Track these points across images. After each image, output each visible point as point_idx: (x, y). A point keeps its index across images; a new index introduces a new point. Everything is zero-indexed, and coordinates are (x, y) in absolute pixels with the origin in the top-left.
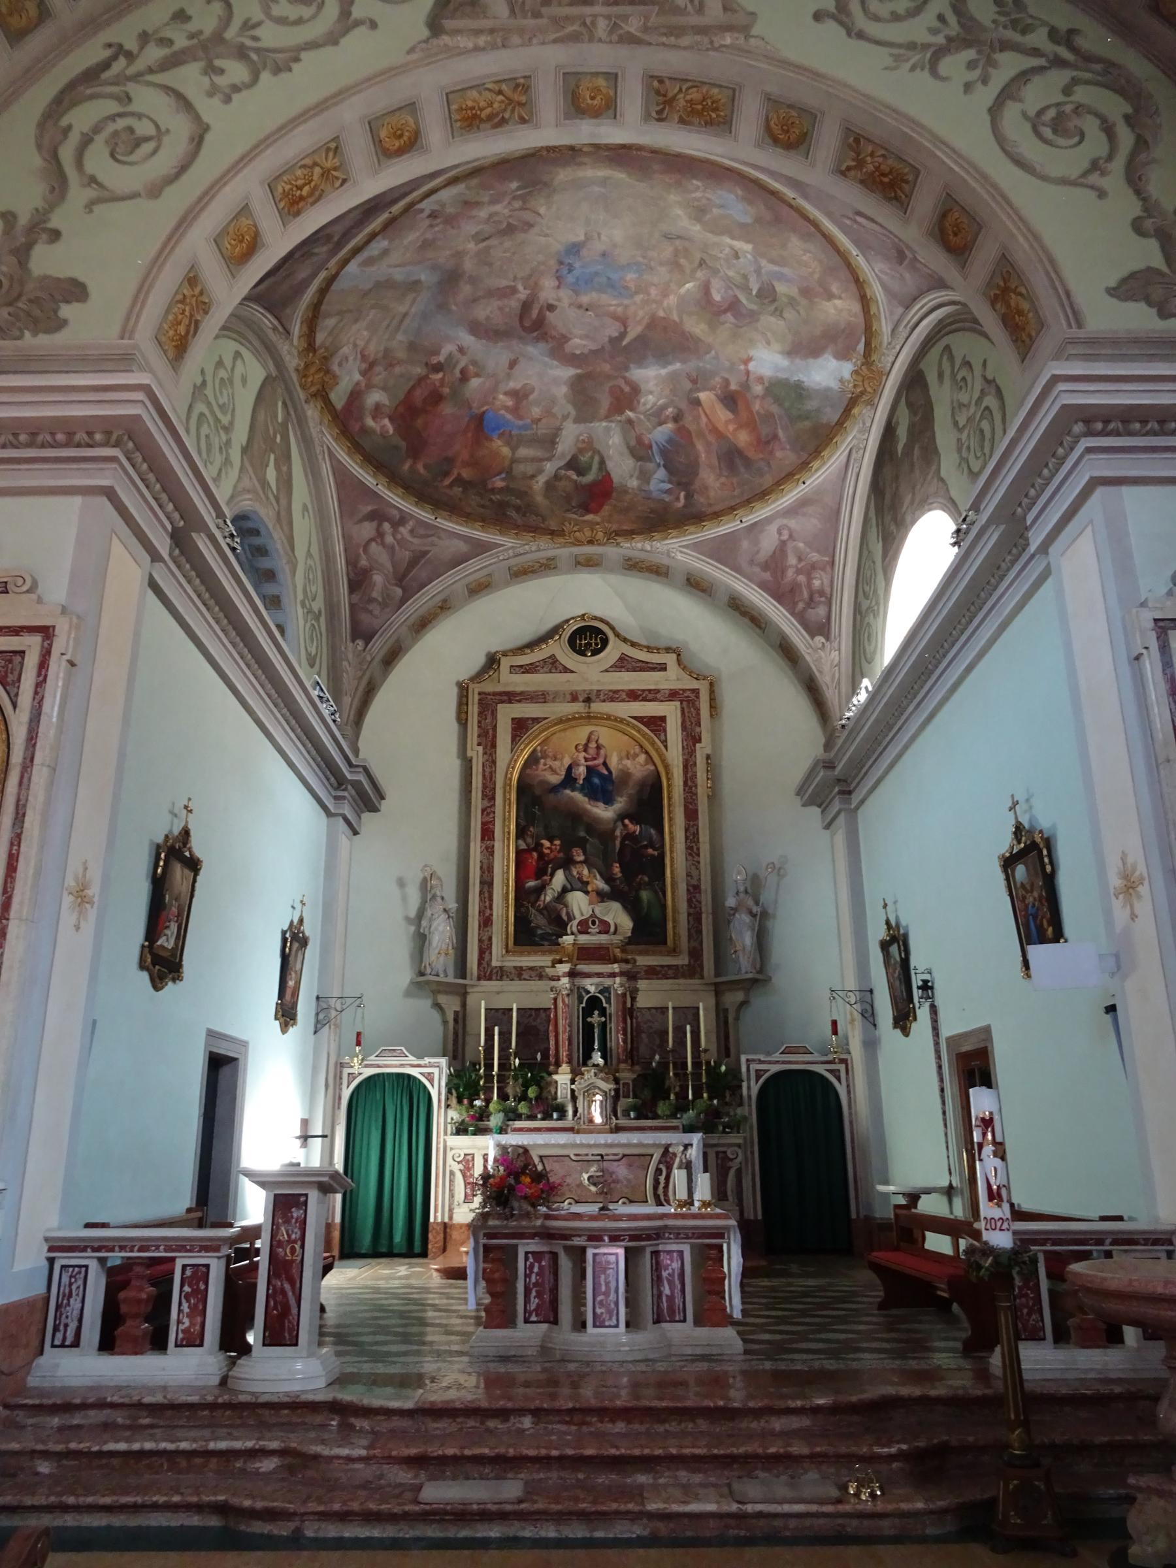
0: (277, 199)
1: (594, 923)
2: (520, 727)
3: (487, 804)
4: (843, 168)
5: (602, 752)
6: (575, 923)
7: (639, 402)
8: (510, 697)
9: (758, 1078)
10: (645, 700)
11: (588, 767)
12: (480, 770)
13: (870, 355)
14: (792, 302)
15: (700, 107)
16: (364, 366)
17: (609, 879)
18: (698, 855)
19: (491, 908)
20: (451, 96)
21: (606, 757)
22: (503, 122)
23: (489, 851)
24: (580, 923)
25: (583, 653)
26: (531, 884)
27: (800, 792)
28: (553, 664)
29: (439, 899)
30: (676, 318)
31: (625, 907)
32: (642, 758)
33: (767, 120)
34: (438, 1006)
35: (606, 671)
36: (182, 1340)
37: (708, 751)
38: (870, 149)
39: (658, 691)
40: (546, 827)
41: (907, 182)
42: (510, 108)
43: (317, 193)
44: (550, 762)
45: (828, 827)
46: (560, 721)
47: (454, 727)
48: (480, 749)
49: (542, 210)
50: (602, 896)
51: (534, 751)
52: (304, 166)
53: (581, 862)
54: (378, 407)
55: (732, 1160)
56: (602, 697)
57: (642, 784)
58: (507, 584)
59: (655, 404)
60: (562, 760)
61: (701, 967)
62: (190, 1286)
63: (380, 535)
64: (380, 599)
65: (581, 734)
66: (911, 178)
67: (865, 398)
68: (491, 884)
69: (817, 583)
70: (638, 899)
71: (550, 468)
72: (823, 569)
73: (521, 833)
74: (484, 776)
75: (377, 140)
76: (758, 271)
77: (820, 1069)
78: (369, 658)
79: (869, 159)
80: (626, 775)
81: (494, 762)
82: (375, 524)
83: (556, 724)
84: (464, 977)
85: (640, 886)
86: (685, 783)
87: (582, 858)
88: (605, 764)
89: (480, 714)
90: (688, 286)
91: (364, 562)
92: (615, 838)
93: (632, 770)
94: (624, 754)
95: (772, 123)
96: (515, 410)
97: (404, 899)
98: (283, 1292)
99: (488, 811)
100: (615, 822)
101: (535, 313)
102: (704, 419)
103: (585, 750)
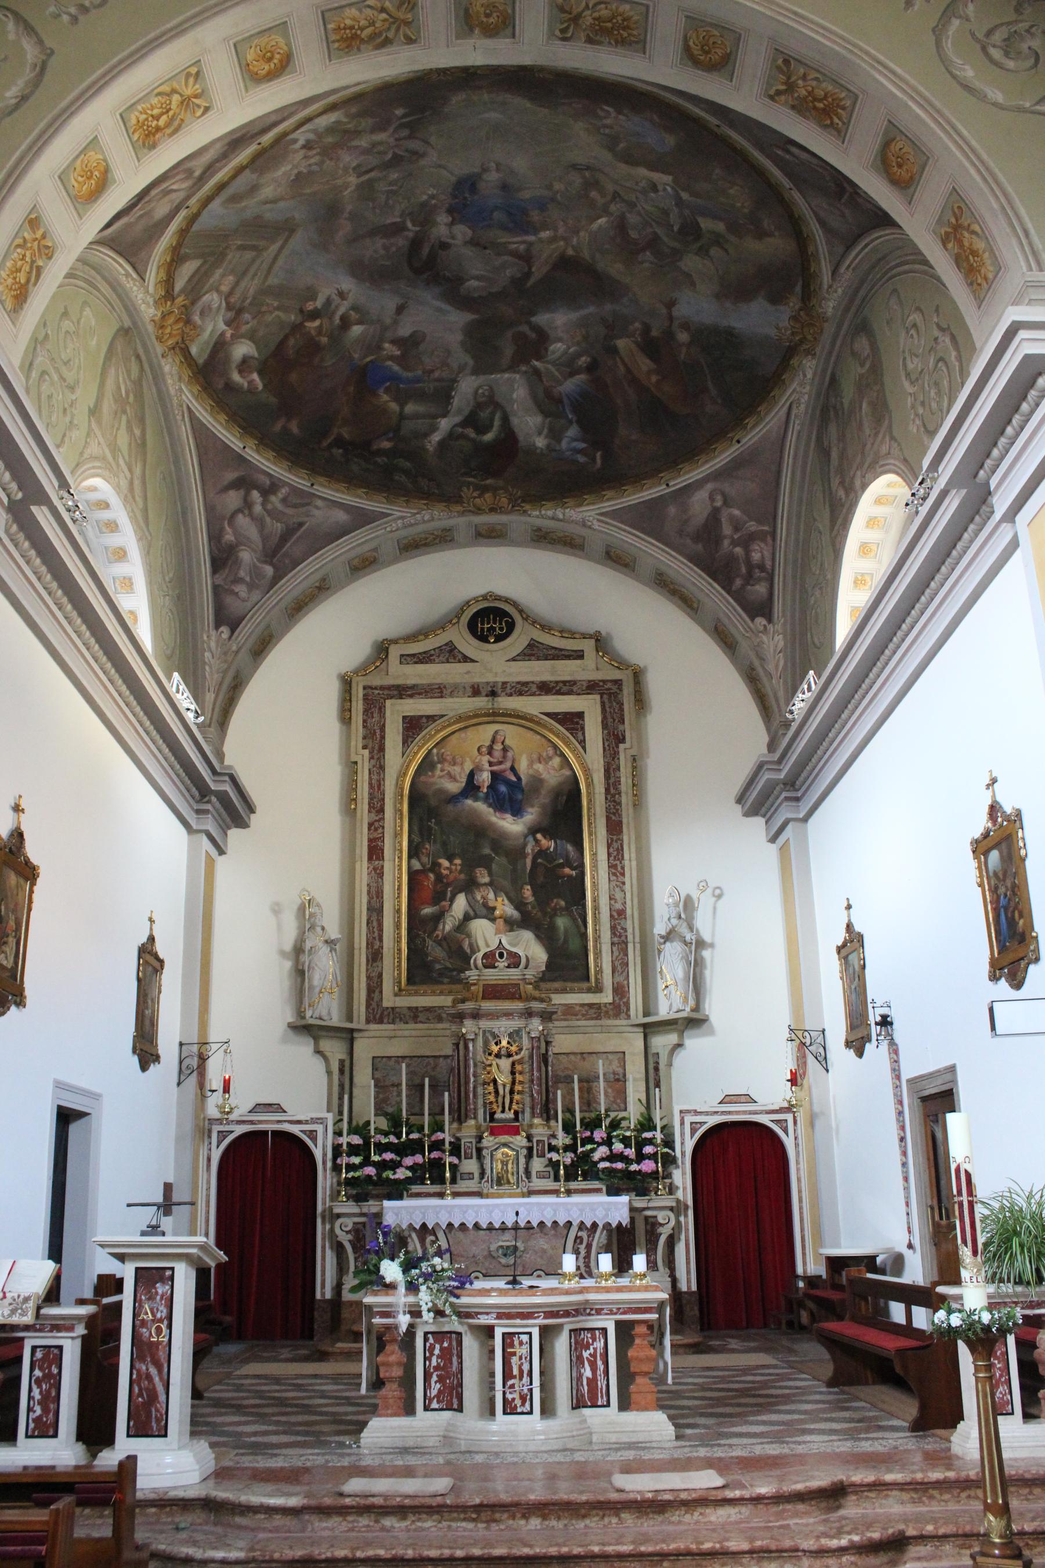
0: (131, 131)
1: (501, 955)
2: (413, 726)
3: (374, 817)
4: (772, 92)
5: (510, 754)
6: (480, 955)
7: (546, 350)
8: (402, 691)
9: (693, 1131)
10: (559, 693)
11: (493, 773)
12: (366, 777)
13: (809, 300)
14: (718, 240)
15: (609, 25)
16: (230, 315)
17: (519, 904)
18: (623, 874)
19: (381, 940)
20: (327, 15)
21: (513, 761)
22: (387, 42)
23: (378, 873)
24: (486, 956)
25: (484, 639)
26: (427, 910)
27: (740, 800)
28: (450, 653)
29: (319, 929)
30: (586, 254)
31: (538, 937)
32: (557, 761)
33: (686, 39)
34: (318, 1052)
35: (513, 659)
36: (34, 1430)
37: (633, 752)
38: (802, 71)
39: (574, 683)
40: (444, 844)
41: (844, 108)
42: (394, 27)
43: (176, 123)
44: (448, 768)
45: (773, 840)
46: (460, 719)
47: (334, 726)
48: (366, 752)
49: (433, 140)
50: (511, 925)
51: (430, 752)
52: (159, 94)
53: (485, 884)
54: (245, 360)
55: (662, 1225)
56: (508, 691)
57: (557, 793)
58: (395, 560)
59: (566, 352)
61: (627, 1005)
62: (40, 1369)
63: (248, 505)
64: (248, 579)
65: (485, 734)
66: (848, 103)
67: (805, 347)
68: (380, 911)
69: (756, 556)
70: (553, 928)
71: (445, 424)
72: (764, 540)
73: (414, 852)
74: (370, 784)
75: (244, 63)
76: (679, 202)
77: (764, 1119)
78: (234, 648)
79: (800, 82)
80: (537, 782)
81: (382, 768)
82: (242, 492)
83: (454, 723)
84: (352, 1022)
85: (555, 912)
86: (607, 790)
87: (487, 880)
88: (513, 769)
89: (366, 711)
90: (602, 221)
91: (229, 537)
92: (524, 856)
93: (545, 776)
94: (535, 756)
95: (691, 43)
96: (402, 360)
97: (279, 927)
98: (149, 1377)
99: (376, 826)
100: (526, 836)
101: (425, 251)
102: (622, 369)
103: (490, 753)
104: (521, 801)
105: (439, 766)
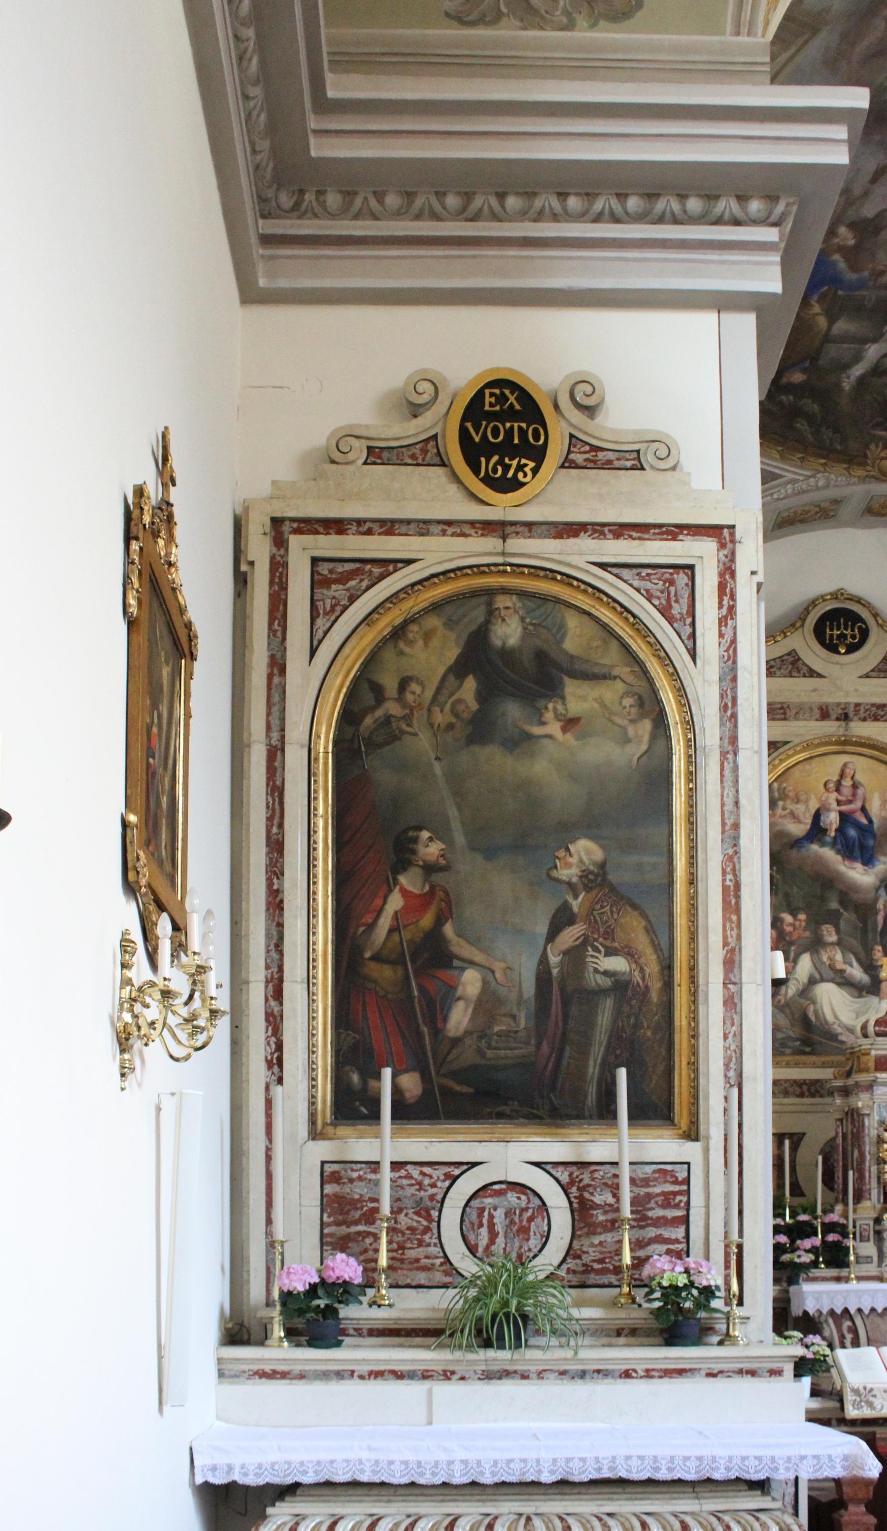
11: (841, 814)
44: (791, 806)
60: (806, 802)
88: (863, 809)
103: (838, 790)
104: (873, 848)
105: (781, 803)
